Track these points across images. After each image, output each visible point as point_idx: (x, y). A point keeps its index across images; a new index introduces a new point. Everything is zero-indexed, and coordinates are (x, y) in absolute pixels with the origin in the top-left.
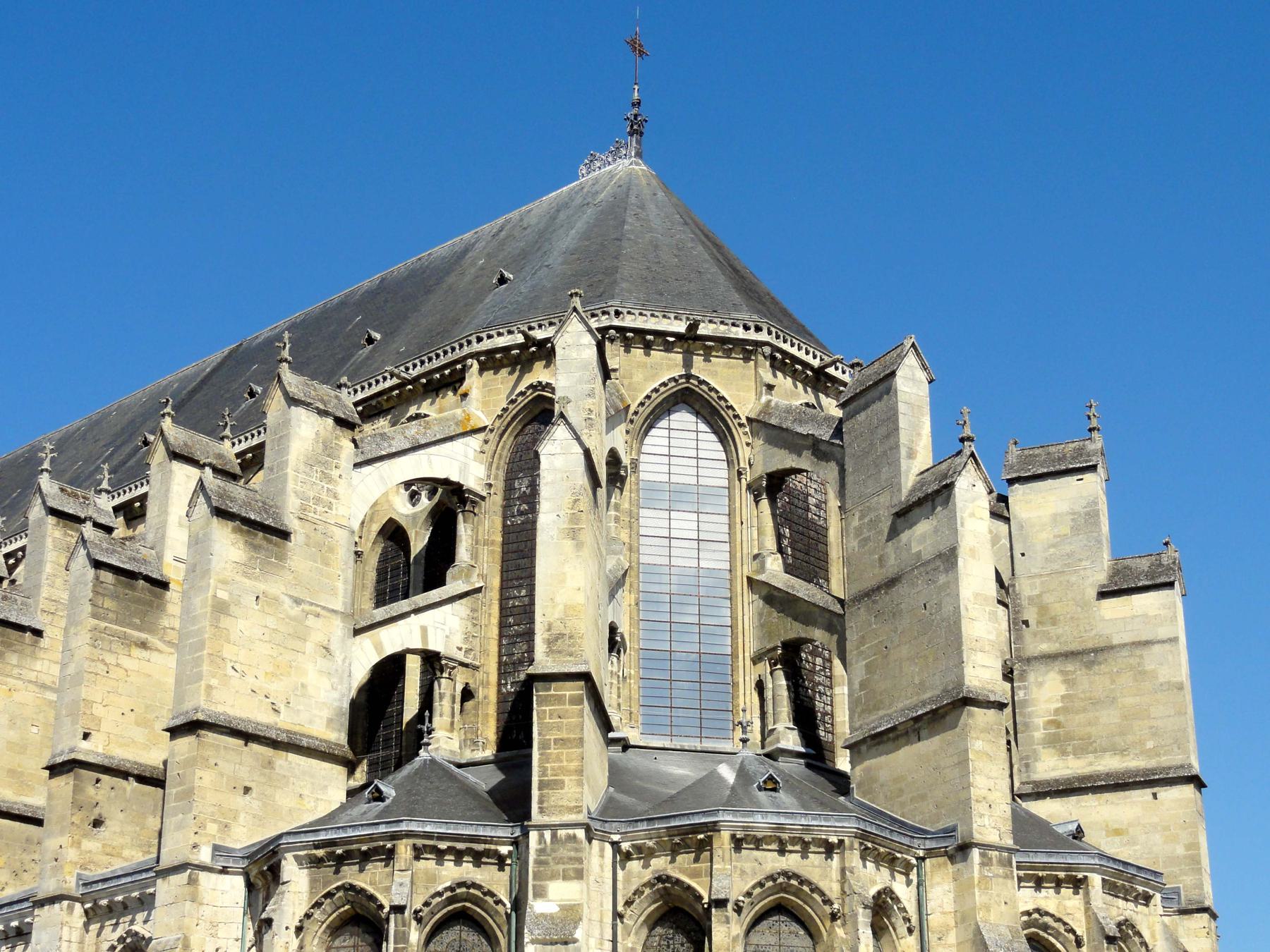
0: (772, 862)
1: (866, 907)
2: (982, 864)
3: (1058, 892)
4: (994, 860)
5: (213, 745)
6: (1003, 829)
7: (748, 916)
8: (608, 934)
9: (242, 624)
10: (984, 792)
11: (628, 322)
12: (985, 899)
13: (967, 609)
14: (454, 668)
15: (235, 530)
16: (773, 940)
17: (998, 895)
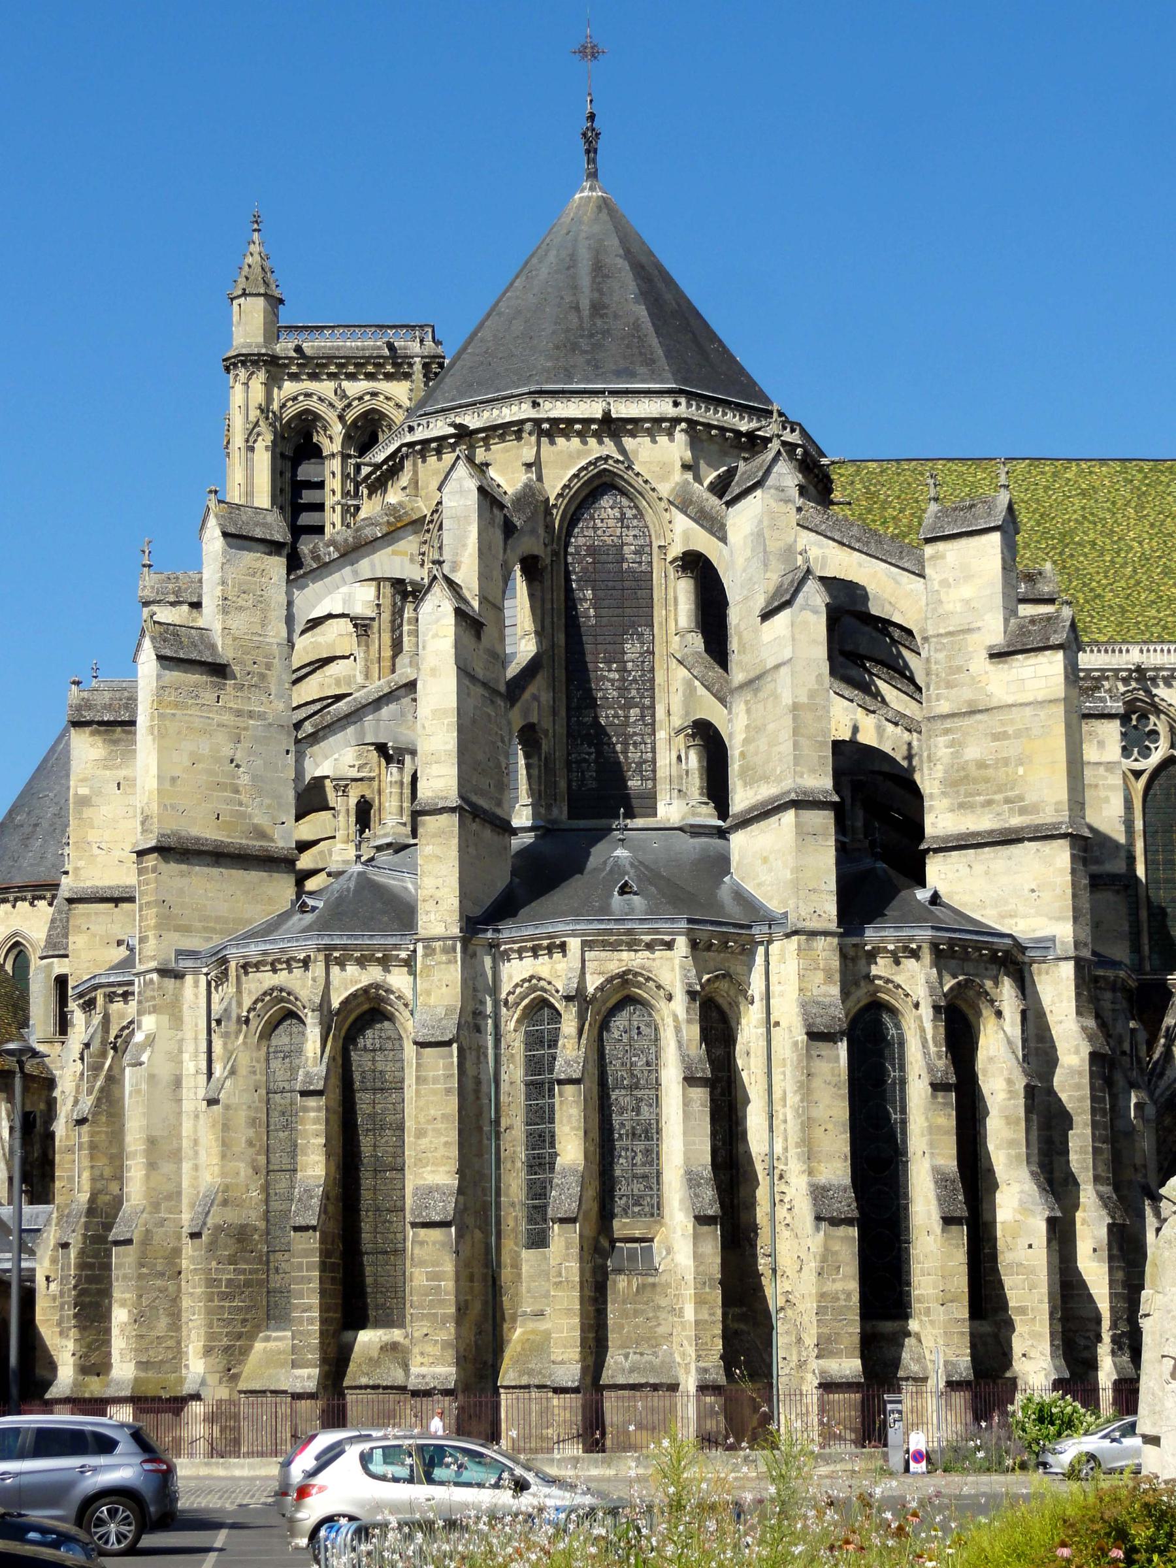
0: (268, 979)
1: (313, 1011)
2: (425, 956)
3: (551, 958)
4: (438, 950)
5: (84, 914)
6: (449, 921)
7: (257, 1025)
8: (203, 1047)
9: (104, 810)
10: (432, 891)
11: (420, 434)
12: (426, 985)
13: (424, 727)
14: (347, 785)
15: (93, 734)
16: (286, 1040)
17: (440, 980)
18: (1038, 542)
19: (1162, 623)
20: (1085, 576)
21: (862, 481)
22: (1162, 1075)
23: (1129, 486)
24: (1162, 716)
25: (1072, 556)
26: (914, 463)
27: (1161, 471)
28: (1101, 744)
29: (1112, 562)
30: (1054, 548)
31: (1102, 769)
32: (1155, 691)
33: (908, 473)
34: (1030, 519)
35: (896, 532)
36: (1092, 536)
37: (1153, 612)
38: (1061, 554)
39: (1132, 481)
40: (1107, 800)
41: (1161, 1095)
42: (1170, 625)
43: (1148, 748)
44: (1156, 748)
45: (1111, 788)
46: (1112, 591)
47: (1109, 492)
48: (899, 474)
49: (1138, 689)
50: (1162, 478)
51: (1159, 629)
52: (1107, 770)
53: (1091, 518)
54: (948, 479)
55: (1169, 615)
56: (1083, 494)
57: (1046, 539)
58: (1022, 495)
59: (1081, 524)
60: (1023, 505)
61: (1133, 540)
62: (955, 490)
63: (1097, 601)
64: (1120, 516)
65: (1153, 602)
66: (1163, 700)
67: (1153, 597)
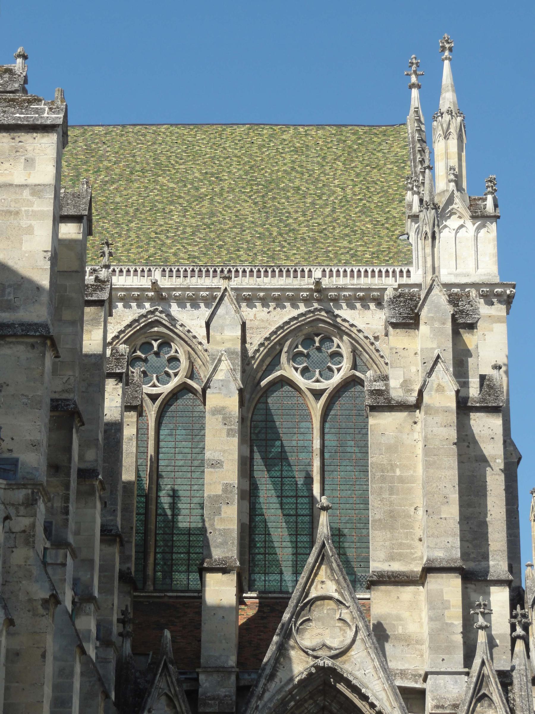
18: (243, 187)
19: (352, 252)
20: (283, 214)
21: (85, 140)
22: (272, 676)
23: (341, 145)
24: (345, 338)
25: (274, 198)
26: (138, 127)
27: (375, 134)
28: (29, 162)
29: (313, 203)
30: (258, 192)
31: (26, 193)
32: (337, 312)
33: (131, 135)
34: (239, 170)
35: (107, 179)
36: (297, 183)
37: (345, 243)
38: (263, 196)
39: (345, 141)
40: (30, 230)
41: (270, 700)
42: (359, 253)
43: (330, 369)
44: (339, 370)
45: (35, 215)
46: (307, 226)
47: (321, 149)
48: (122, 135)
49: (320, 310)
50: (375, 139)
51: (348, 257)
52: (33, 194)
53: (299, 169)
54: (168, 139)
55: (361, 245)
56: (296, 151)
57: (251, 185)
58: (236, 151)
59: (289, 174)
60: (235, 159)
61: (338, 186)
62: (172, 147)
63: (291, 234)
64: (327, 168)
65: (347, 235)
66: (345, 320)
67: (347, 231)
